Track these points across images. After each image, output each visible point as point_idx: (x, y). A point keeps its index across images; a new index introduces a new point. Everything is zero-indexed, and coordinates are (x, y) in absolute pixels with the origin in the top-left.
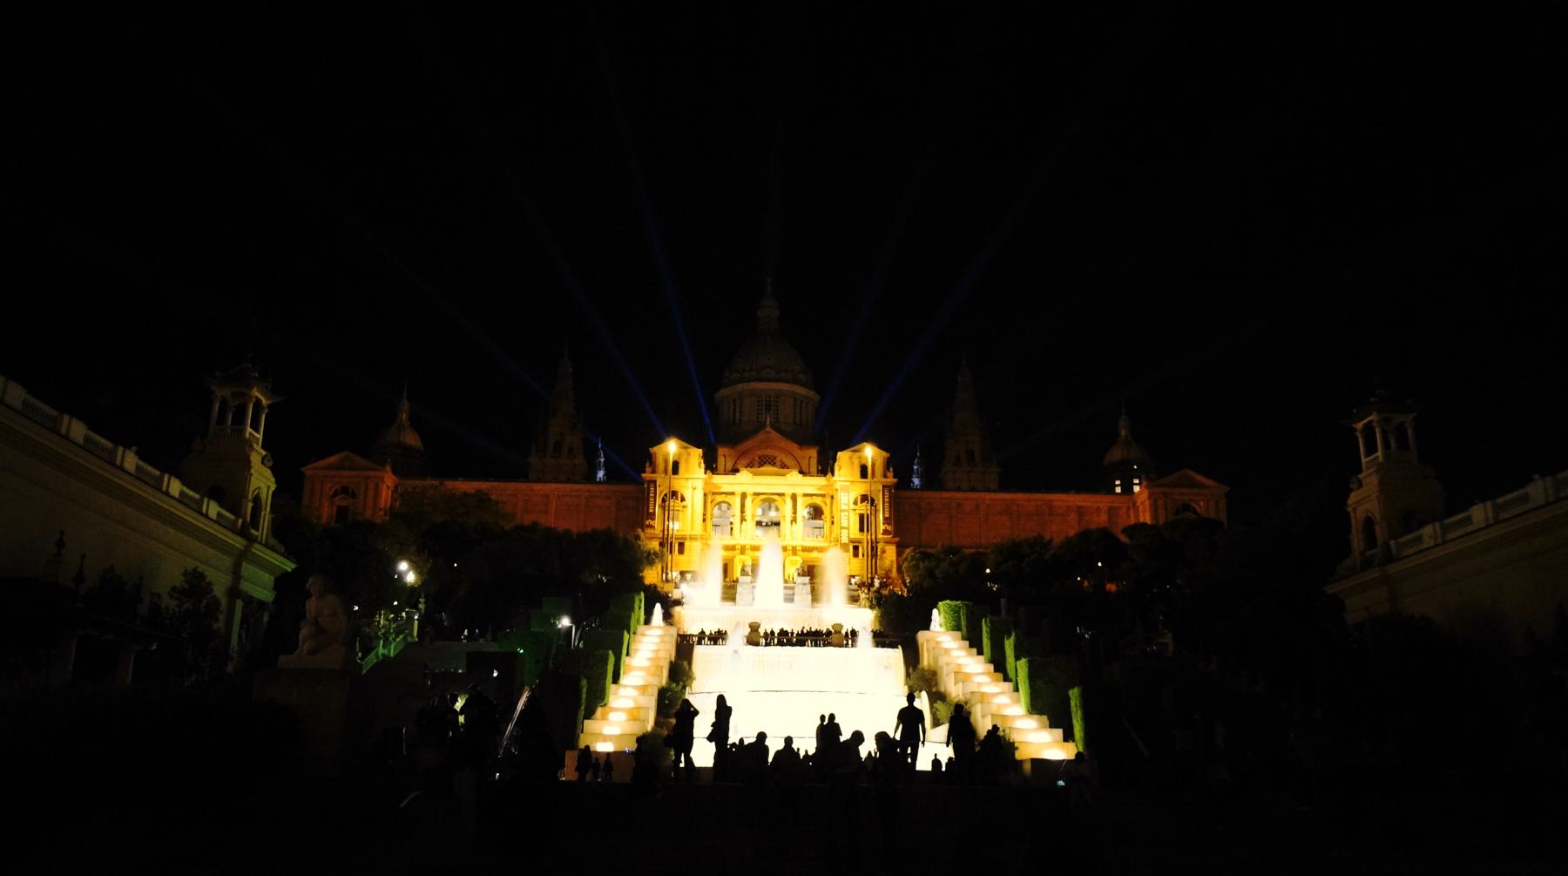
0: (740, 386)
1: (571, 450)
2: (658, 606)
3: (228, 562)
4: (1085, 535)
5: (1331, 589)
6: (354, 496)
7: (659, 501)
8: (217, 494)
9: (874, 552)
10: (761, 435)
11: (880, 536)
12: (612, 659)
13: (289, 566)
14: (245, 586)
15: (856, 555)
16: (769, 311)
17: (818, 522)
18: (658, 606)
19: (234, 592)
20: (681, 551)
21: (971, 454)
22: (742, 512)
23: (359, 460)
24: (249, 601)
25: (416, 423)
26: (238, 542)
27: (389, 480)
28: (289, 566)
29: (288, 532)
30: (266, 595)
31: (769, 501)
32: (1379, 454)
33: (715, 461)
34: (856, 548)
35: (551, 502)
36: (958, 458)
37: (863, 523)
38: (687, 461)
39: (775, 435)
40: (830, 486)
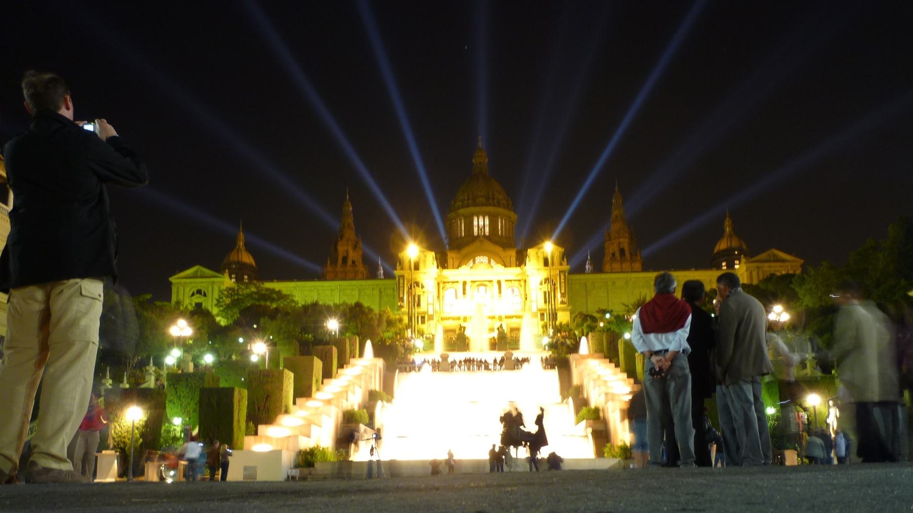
1: (353, 262)
2: (369, 344)
6: (205, 295)
9: (554, 316)
11: (559, 306)
18: (369, 344)
25: (249, 248)
31: (482, 284)
33: (446, 261)
34: (542, 315)
36: (614, 254)
37: (548, 297)
38: (425, 261)
40: (524, 273)
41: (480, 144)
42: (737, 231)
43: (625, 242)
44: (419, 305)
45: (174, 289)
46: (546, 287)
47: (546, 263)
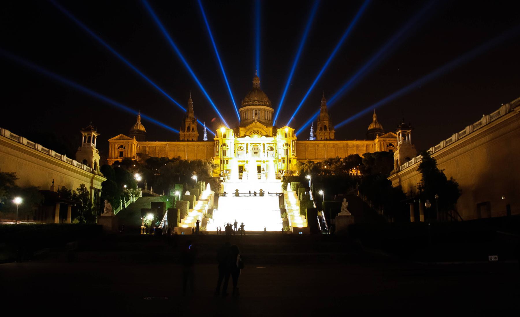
0: (247, 107)
1: (193, 129)
2: (209, 185)
3: (89, 180)
4: (351, 156)
5: (389, 179)
6: (124, 148)
7: (220, 147)
8: (85, 162)
10: (254, 124)
12: (188, 202)
13: (105, 179)
14: (94, 186)
15: (284, 163)
16: (257, 82)
17: (272, 152)
18: (209, 185)
19: (91, 188)
20: (227, 163)
21: (325, 127)
22: (247, 149)
23: (125, 137)
24: (95, 189)
25: (143, 123)
26: (92, 175)
27: (135, 142)
28: (105, 179)
29: (105, 169)
30: (100, 188)
32: (401, 141)
33: (239, 132)
34: (284, 160)
35: (184, 150)
37: (287, 152)
38: (228, 134)
39: (259, 124)
40: (275, 140)
41: (257, 73)
42: (379, 120)
43: (327, 123)
44: (225, 155)
45: (110, 146)
46: (286, 147)
47: (286, 136)
